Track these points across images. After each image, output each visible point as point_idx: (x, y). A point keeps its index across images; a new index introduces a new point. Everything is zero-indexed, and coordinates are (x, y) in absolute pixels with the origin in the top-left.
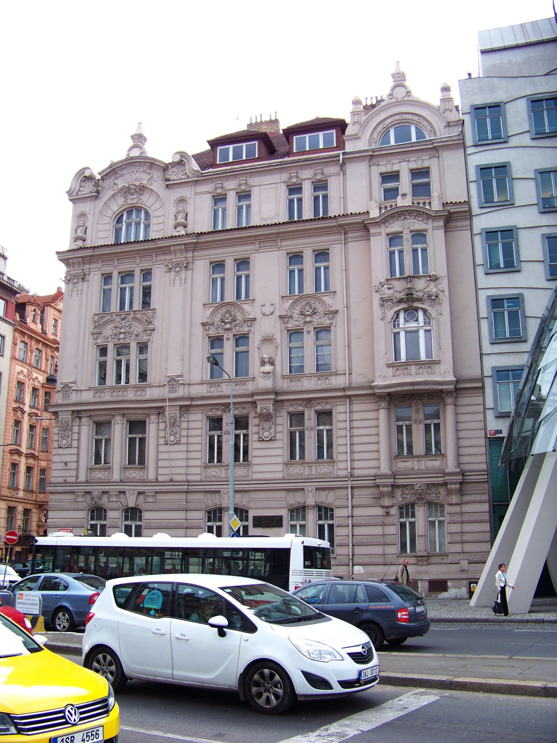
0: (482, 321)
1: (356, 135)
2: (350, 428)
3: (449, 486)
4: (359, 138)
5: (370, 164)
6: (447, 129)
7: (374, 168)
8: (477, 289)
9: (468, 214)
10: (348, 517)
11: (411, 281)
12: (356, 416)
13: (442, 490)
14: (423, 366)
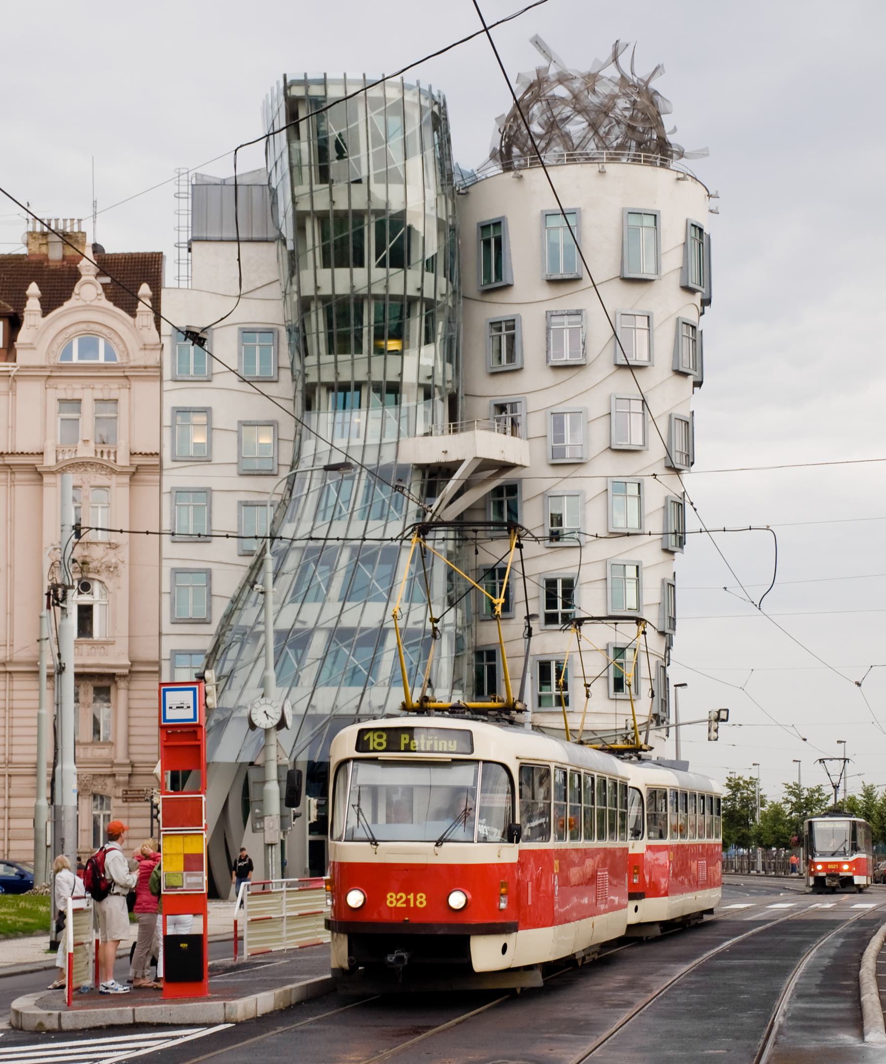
0: (163, 595)
1: (32, 344)
2: (9, 709)
3: (117, 778)
4: (35, 348)
5: (47, 386)
6: (143, 352)
7: (50, 391)
8: (160, 559)
9: (159, 467)
10: (5, 808)
11: (88, 547)
12: (16, 695)
13: (109, 781)
14: (96, 646)
